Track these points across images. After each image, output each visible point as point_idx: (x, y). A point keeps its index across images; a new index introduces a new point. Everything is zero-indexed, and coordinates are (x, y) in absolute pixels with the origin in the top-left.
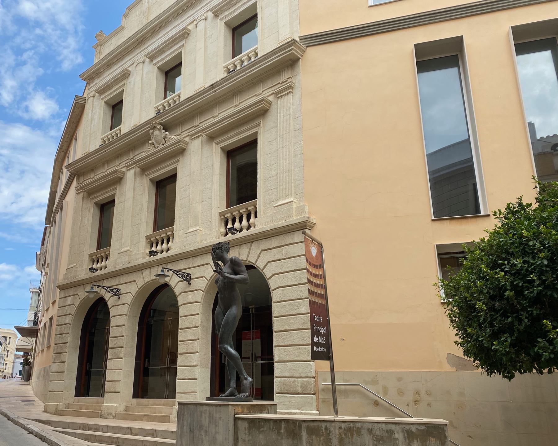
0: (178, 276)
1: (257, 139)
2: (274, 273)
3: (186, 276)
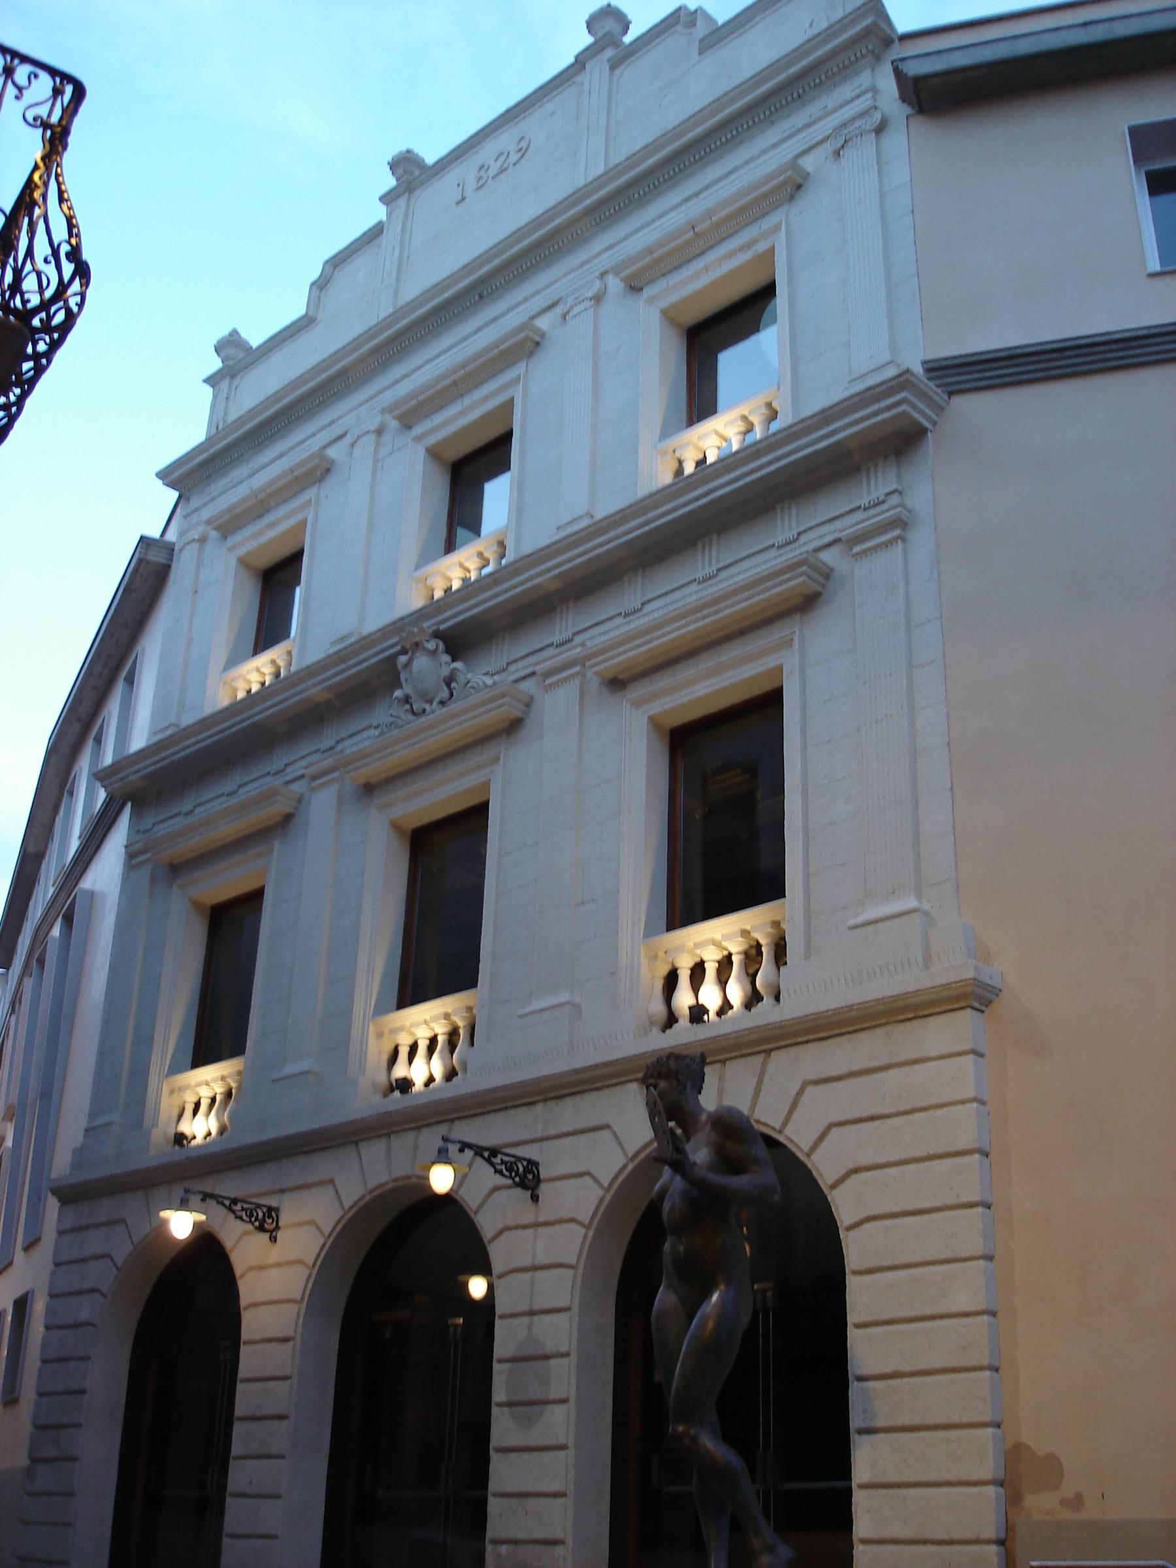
0: (496, 1171)
1: (782, 687)
2: (851, 1166)
3: (521, 1169)
